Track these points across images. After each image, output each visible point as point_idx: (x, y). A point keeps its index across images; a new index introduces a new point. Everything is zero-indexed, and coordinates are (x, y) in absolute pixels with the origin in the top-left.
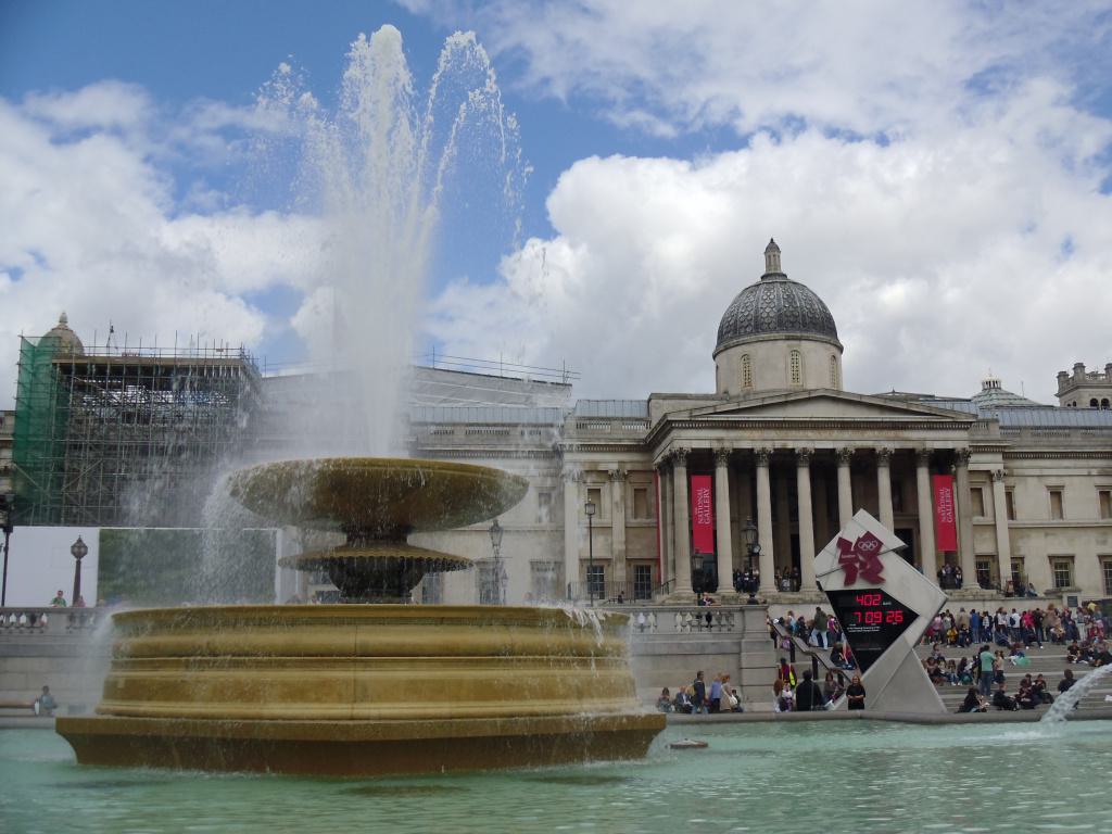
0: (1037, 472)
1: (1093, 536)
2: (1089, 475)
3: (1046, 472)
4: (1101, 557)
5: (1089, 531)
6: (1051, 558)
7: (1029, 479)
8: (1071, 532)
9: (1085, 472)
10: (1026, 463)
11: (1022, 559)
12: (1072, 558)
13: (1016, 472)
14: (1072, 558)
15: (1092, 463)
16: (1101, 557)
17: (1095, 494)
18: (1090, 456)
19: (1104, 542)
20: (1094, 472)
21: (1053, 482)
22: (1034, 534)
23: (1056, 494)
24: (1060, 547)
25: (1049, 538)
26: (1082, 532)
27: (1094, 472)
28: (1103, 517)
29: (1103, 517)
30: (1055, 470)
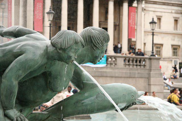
0: (153, 9)
1: (170, 37)
2: (172, 13)
3: (157, 10)
4: (172, 46)
7: (150, 12)
9: (170, 11)
12: (162, 45)
13: (147, 9)
14: (162, 45)
16: (172, 46)
17: (173, 21)
18: (173, 5)
19: (174, 40)
20: (173, 11)
21: (159, 14)
26: (166, 35)
28: (174, 30)
29: (174, 30)
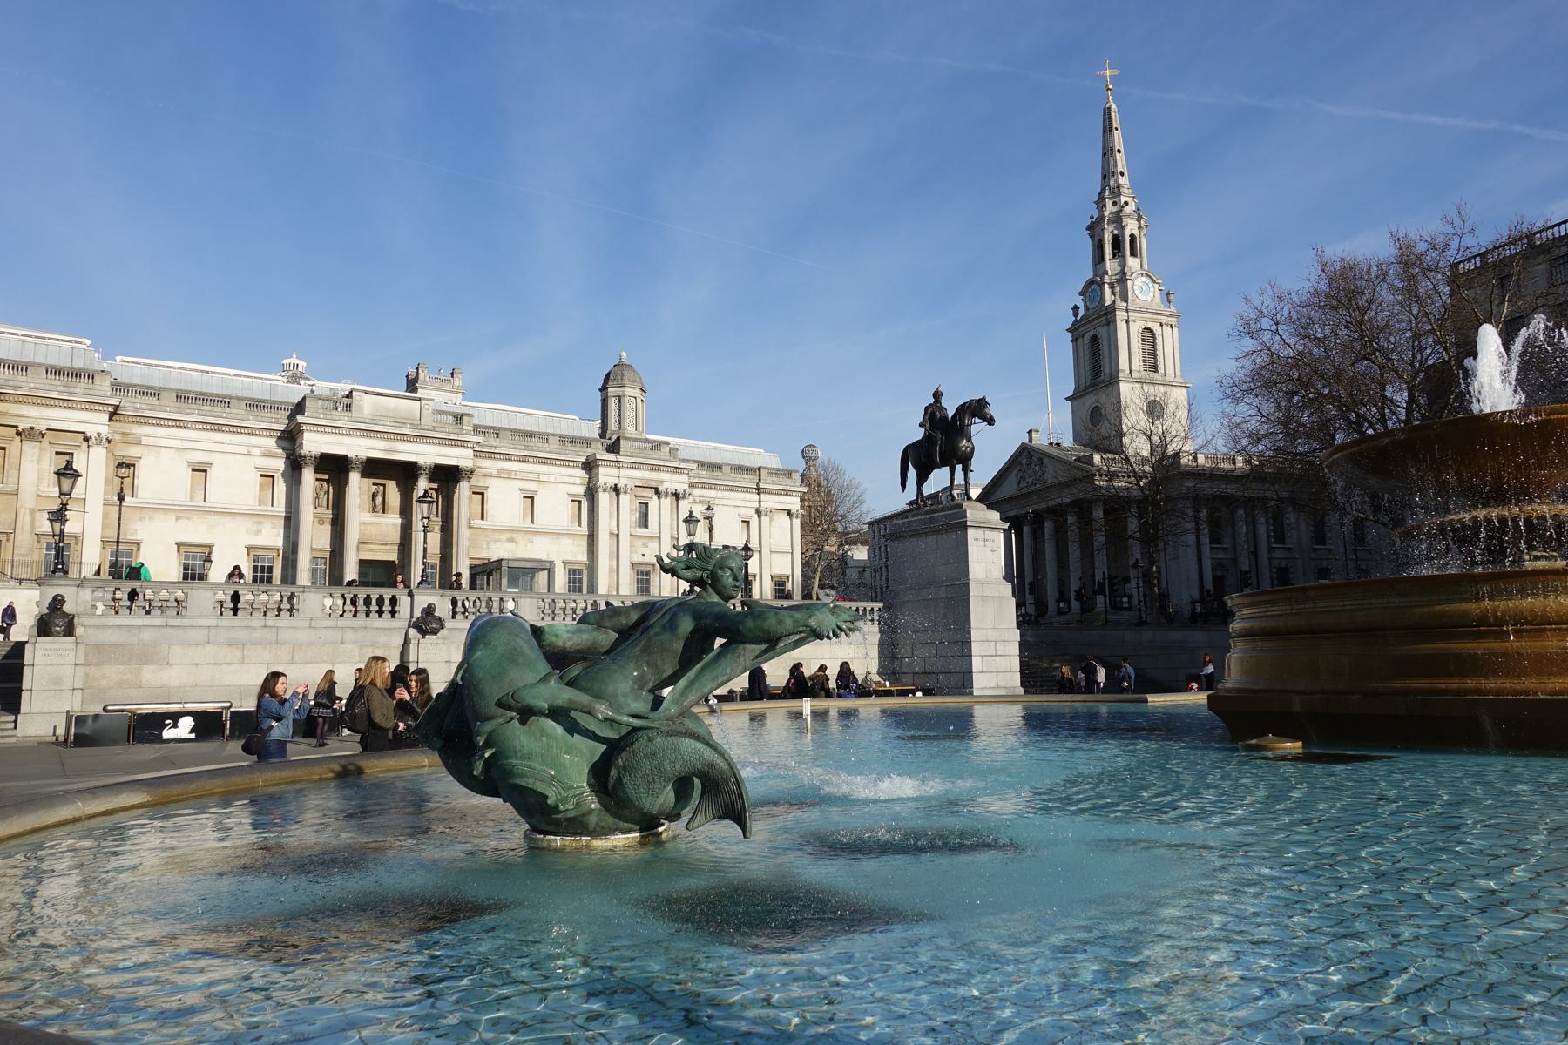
2: (249, 454)
4: (249, 548)
5: (239, 518)
6: (179, 545)
8: (213, 518)
10: (161, 431)
11: (138, 544)
13: (144, 440)
15: (254, 440)
16: (249, 548)
18: (252, 432)
19: (258, 533)
22: (159, 516)
23: (201, 470)
24: (196, 532)
25: (182, 522)
26: (229, 518)
27: (256, 451)
30: (202, 444)
